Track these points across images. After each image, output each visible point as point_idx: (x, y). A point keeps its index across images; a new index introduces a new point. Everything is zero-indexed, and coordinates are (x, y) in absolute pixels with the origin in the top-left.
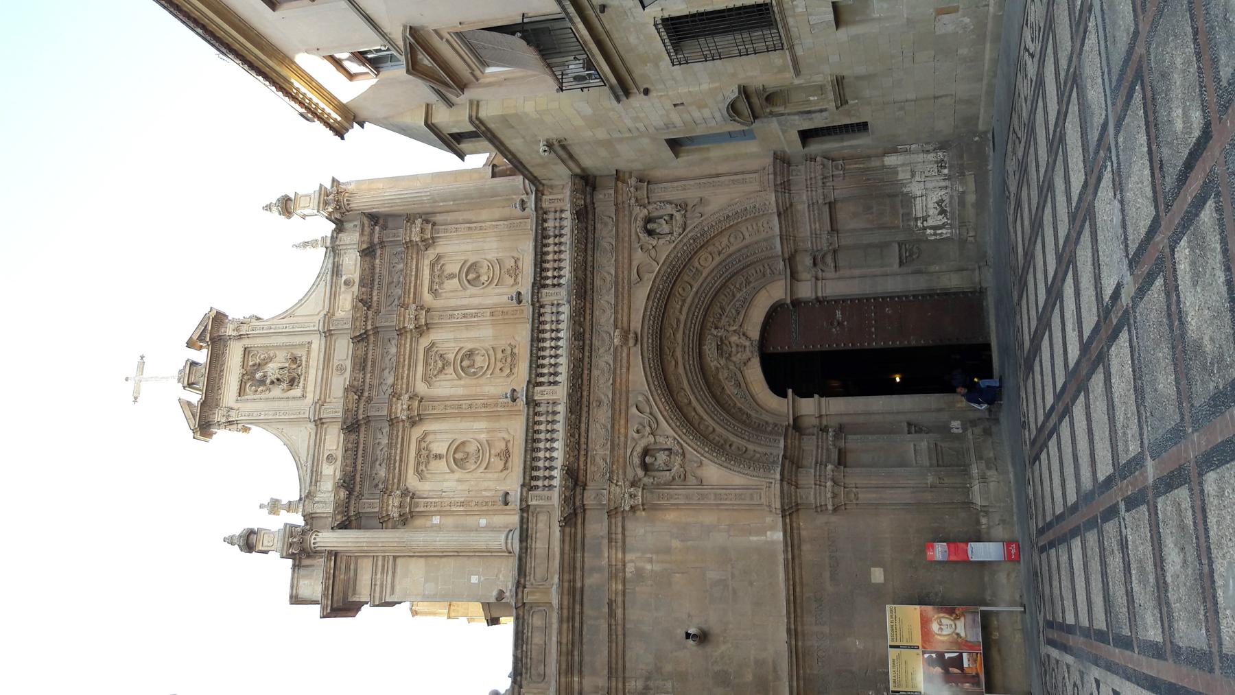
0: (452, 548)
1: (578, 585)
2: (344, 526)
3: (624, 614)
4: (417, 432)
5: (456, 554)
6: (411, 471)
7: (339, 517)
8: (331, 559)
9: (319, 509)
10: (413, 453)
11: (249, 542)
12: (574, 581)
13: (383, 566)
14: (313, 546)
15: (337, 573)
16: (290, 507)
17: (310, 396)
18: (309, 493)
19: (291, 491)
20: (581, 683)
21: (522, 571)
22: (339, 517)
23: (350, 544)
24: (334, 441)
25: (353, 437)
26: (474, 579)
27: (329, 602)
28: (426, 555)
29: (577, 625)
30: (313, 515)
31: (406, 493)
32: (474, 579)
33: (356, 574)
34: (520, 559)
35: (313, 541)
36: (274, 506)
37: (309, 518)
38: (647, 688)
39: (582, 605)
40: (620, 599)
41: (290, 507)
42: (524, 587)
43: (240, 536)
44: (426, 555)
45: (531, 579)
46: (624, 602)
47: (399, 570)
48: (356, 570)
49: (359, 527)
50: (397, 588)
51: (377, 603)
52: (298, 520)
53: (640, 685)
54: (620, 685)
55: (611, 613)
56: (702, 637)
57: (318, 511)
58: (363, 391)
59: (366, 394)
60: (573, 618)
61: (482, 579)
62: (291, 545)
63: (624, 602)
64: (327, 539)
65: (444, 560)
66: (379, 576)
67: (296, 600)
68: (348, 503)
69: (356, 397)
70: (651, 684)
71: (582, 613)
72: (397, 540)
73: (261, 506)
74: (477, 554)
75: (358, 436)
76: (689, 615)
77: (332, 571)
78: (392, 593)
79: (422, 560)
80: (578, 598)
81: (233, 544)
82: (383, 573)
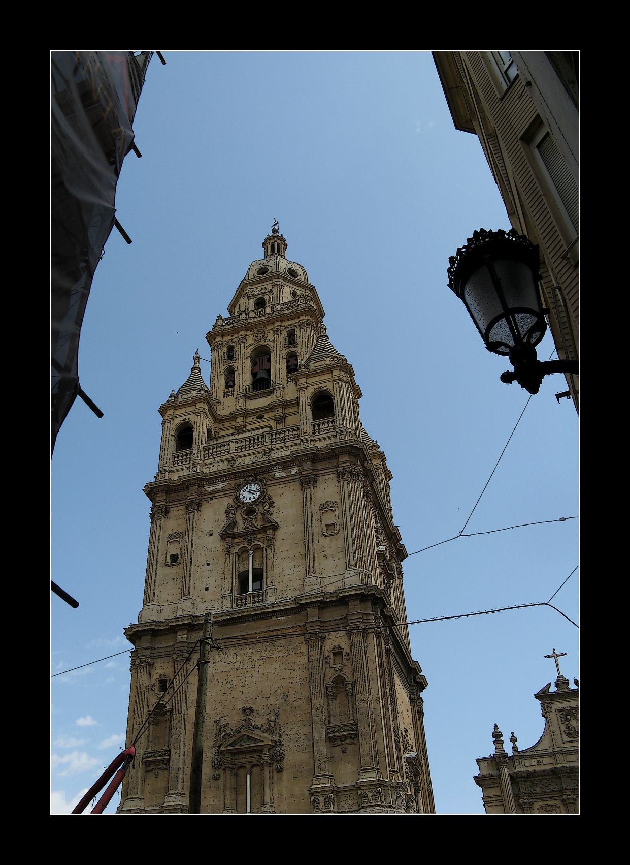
4: (558, 803)
6: (541, 803)
10: (549, 803)
11: (497, 735)
16: (515, 748)
17: (565, 745)
19: (522, 746)
22: (515, 775)
24: (547, 764)
25: (551, 773)
31: (531, 804)
36: (513, 740)
58: (572, 773)
59: (571, 775)
64: (506, 772)
69: (568, 771)
73: (513, 733)
75: (551, 775)
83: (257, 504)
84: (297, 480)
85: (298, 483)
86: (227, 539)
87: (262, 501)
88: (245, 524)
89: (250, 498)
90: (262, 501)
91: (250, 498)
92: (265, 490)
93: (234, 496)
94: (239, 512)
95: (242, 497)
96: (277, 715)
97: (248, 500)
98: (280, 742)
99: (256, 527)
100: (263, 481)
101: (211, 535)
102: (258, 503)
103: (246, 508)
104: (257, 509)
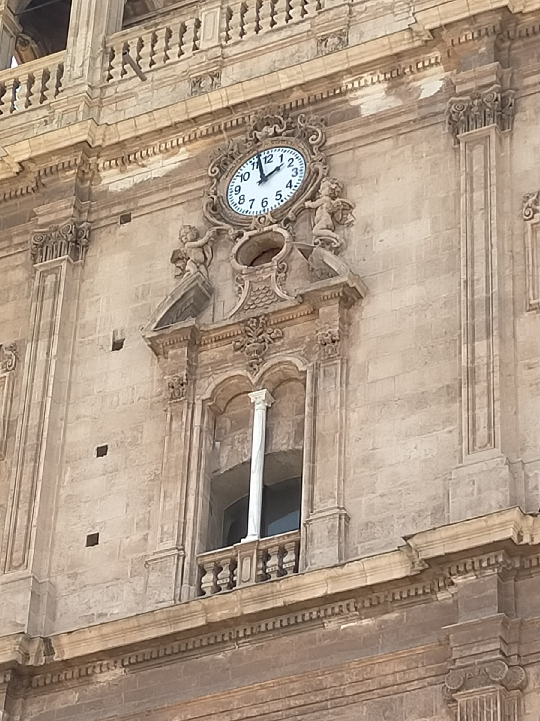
83: (287, 221)
84: (439, 119)
85: (443, 130)
86: (171, 352)
87: (308, 204)
88: (243, 297)
89: (264, 202)
90: (308, 204)
91: (264, 202)
92: (319, 166)
93: (205, 201)
94: (221, 255)
95: (236, 199)
97: (257, 208)
99: (285, 300)
100: (314, 132)
101: (117, 346)
102: (290, 215)
103: (246, 235)
104: (286, 234)
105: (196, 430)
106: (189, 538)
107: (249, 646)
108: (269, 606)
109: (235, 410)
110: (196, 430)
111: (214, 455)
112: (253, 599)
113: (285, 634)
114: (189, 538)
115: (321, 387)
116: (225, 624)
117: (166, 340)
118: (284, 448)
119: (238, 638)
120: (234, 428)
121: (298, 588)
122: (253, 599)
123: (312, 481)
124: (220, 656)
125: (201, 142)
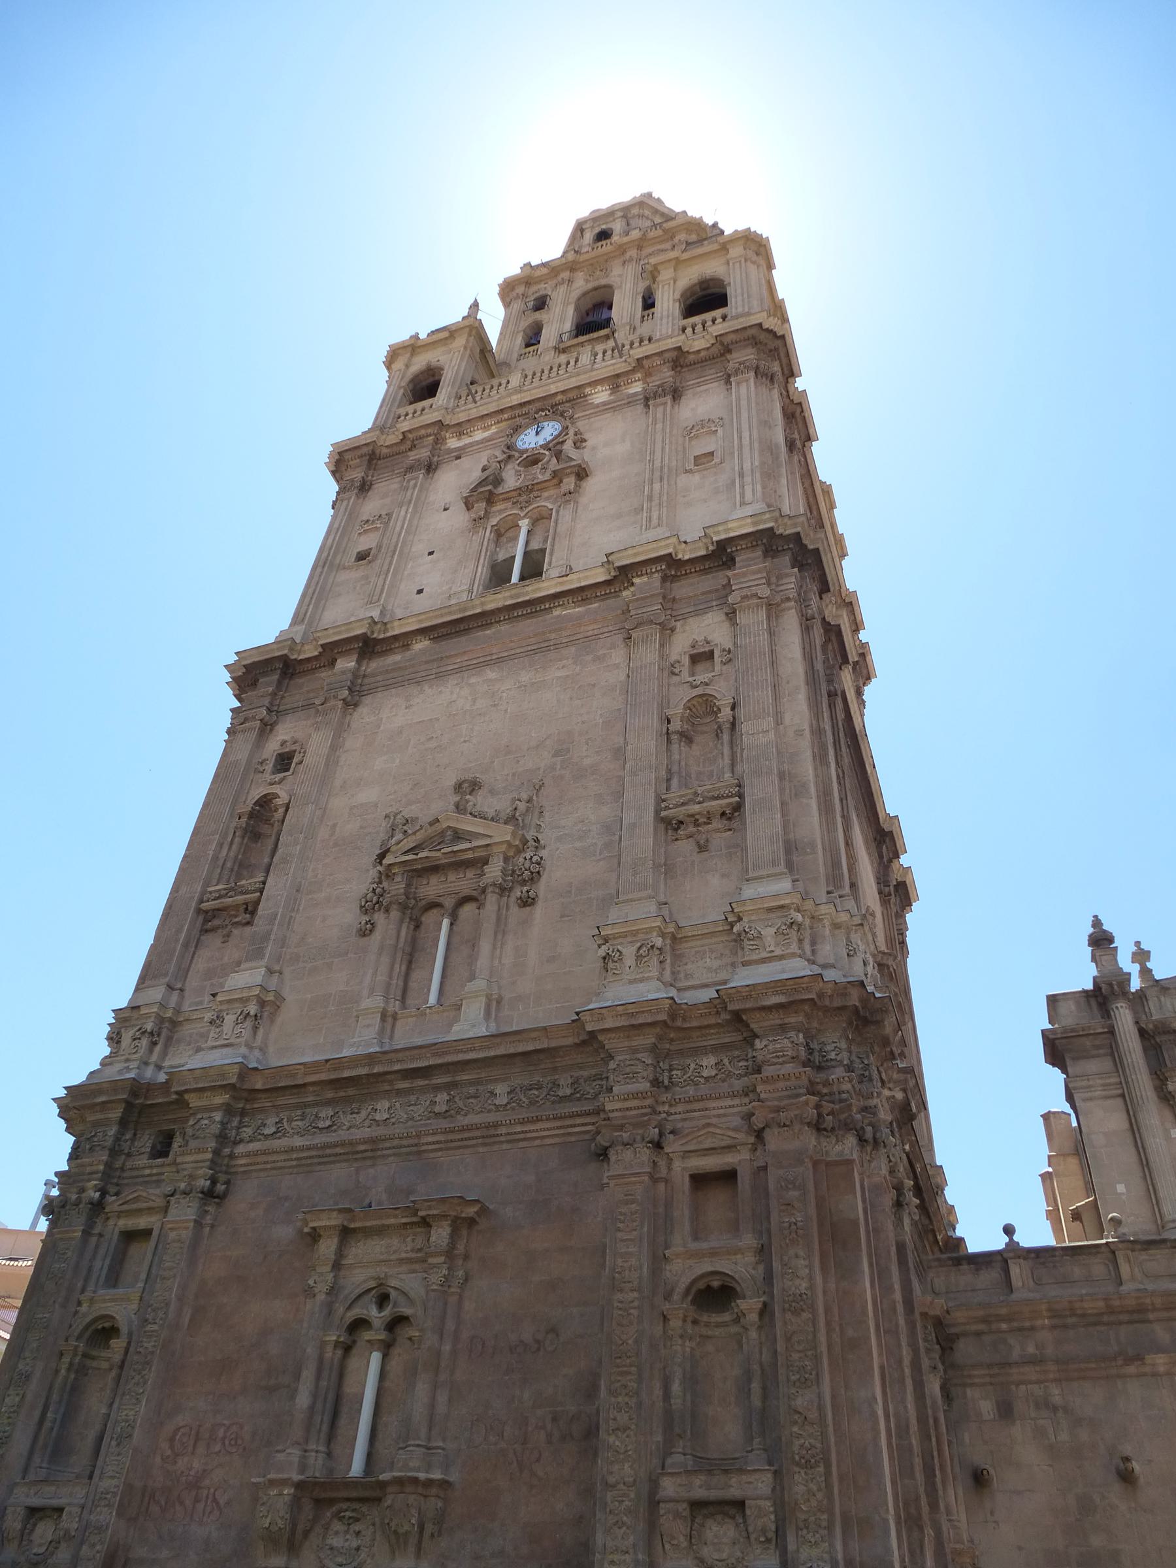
0: (1151, 1159)
1: (1151, 1316)
2: (1142, 1033)
3: (1131, 1376)
5: (1145, 1163)
7: (1151, 1026)
8: (1103, 1028)
9: (1152, 1005)
12: (1155, 1310)
13: (1110, 1084)
14: (1114, 1006)
15: (1091, 1037)
16: (1146, 972)
18: (1168, 989)
20: (1043, 1327)
21: (1149, 1244)
23: (1125, 1045)
26: (1121, 1188)
27: (1059, 1036)
28: (1135, 1129)
29: (1105, 1319)
30: (1144, 999)
32: (1121, 1188)
33: (1093, 1057)
34: (1164, 1241)
35: (1119, 1005)
36: (1141, 956)
37: (1141, 995)
38: (1055, 1409)
39: (1130, 1322)
40: (1147, 1369)
41: (1146, 972)
42: (1133, 1251)
43: (1105, 931)
44: (1135, 1129)
45: (1143, 1256)
46: (1145, 1374)
47: (1110, 1102)
48: (1098, 1056)
49: (1145, 1050)
50: (1089, 1104)
51: (1070, 1085)
52: (1135, 984)
53: (1057, 1399)
54: (1051, 1376)
55: (1129, 1361)
56: (1127, 1477)
57: (1150, 1003)
60: (1112, 1313)
61: (1124, 1197)
62: (1110, 985)
63: (1145, 1374)
64: (1124, 1018)
65: (1133, 1150)
66: (1099, 1082)
67: (1053, 1000)
68: (1169, 1032)
70: (1060, 1414)
71: (1121, 1323)
72: (1144, 1093)
73: (1138, 943)
74: (1151, 1187)
76: (1150, 1461)
77: (1092, 1032)
78: (1085, 1100)
79: (1126, 1125)
80: (1135, 1317)
81: (1094, 926)
82: (1103, 1085)
96: (539, 788)
98: (537, 840)
105: (486, 540)
106: (476, 585)
107: (507, 626)
108: (520, 600)
109: (510, 534)
110: (486, 540)
111: (495, 553)
112: (511, 597)
113: (529, 618)
114: (476, 585)
115: (561, 513)
116: (493, 612)
117: (474, 498)
118: (537, 548)
119: (500, 621)
120: (508, 542)
121: (539, 589)
122: (511, 597)
123: (552, 554)
124: (488, 632)
125: (504, 423)
